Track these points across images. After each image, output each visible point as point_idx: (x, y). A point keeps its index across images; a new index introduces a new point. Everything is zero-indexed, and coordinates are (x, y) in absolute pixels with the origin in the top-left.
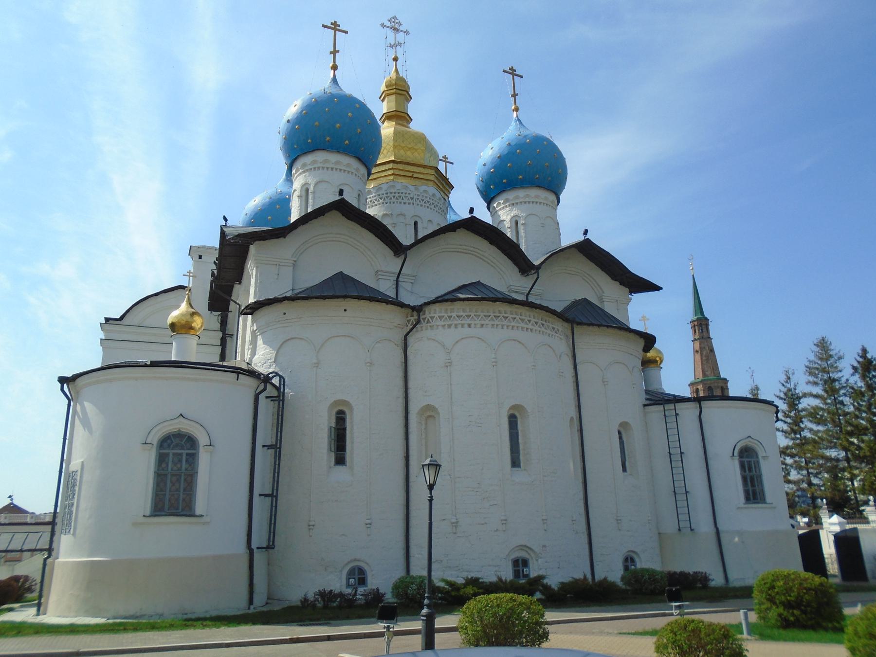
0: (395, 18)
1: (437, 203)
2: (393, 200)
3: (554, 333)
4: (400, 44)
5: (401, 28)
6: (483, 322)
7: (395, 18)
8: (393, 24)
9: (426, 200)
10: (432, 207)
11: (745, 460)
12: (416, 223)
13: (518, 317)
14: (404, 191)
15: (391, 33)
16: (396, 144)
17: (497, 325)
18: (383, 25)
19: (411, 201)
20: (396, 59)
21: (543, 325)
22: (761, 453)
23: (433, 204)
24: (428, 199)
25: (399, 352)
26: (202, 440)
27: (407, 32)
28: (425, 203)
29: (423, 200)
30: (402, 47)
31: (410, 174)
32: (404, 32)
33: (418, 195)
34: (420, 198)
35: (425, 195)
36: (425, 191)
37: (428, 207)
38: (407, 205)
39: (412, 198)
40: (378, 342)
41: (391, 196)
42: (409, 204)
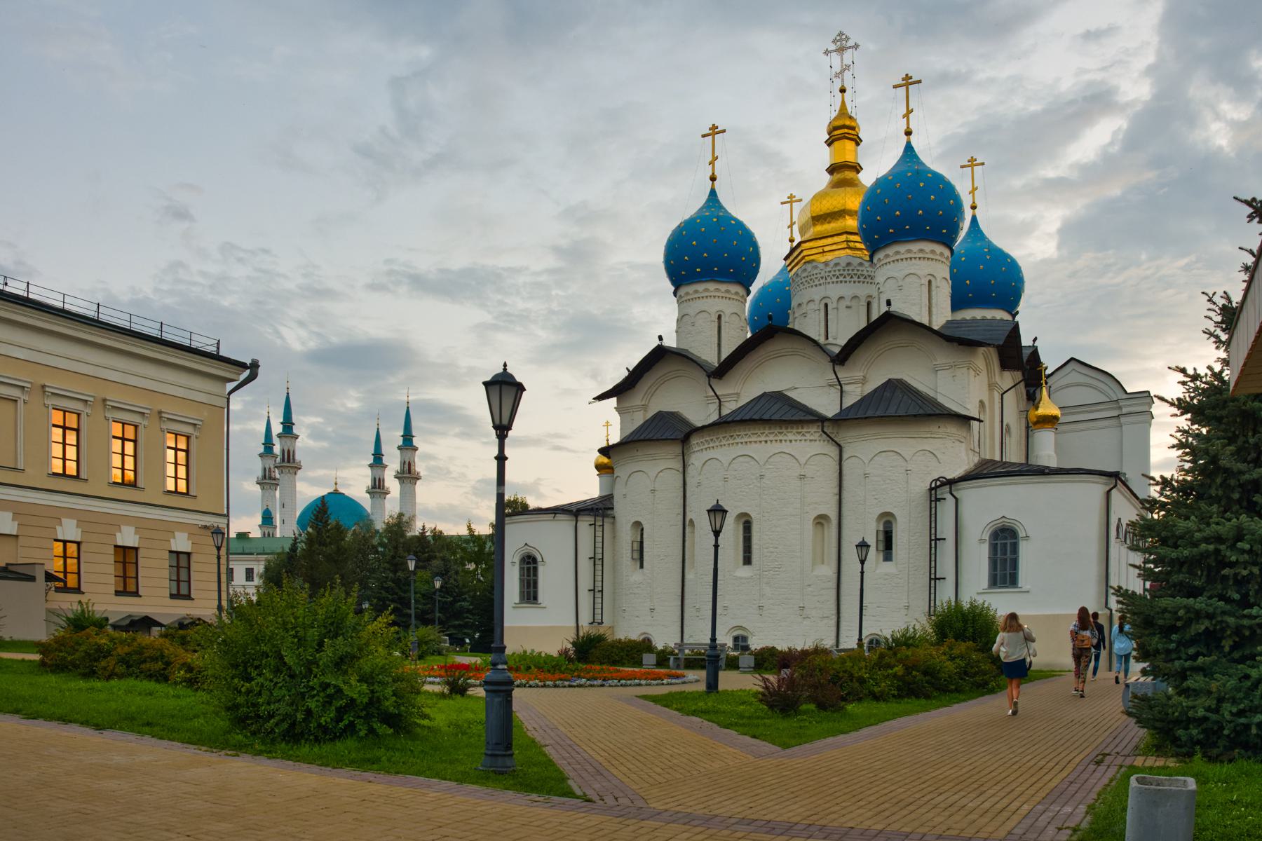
0: (841, 34)
1: (855, 272)
2: (807, 285)
3: (799, 437)
4: (848, 67)
5: (850, 43)
6: (722, 443)
7: (841, 34)
8: (838, 43)
9: (837, 273)
10: (848, 279)
11: (999, 542)
12: (826, 305)
13: (749, 433)
14: (815, 272)
15: (835, 59)
16: (814, 215)
17: (733, 444)
18: (827, 52)
19: (821, 282)
20: (843, 91)
21: (780, 433)
22: (1021, 534)
23: (849, 275)
24: (841, 272)
25: (682, 475)
26: (539, 559)
27: (856, 46)
28: (838, 277)
29: (834, 275)
30: (851, 70)
31: (820, 250)
32: (850, 47)
33: (830, 272)
34: (831, 274)
35: (838, 268)
36: (837, 264)
37: (841, 282)
38: (819, 287)
39: (822, 278)
40: (661, 471)
41: (804, 280)
42: (820, 285)
